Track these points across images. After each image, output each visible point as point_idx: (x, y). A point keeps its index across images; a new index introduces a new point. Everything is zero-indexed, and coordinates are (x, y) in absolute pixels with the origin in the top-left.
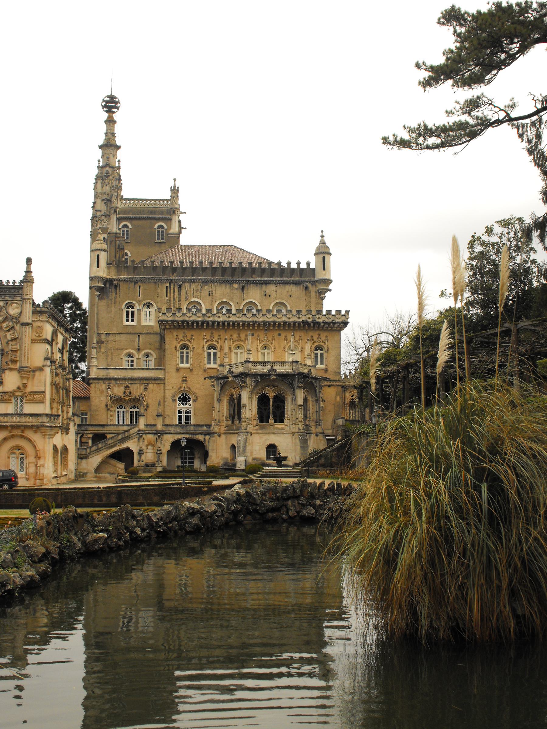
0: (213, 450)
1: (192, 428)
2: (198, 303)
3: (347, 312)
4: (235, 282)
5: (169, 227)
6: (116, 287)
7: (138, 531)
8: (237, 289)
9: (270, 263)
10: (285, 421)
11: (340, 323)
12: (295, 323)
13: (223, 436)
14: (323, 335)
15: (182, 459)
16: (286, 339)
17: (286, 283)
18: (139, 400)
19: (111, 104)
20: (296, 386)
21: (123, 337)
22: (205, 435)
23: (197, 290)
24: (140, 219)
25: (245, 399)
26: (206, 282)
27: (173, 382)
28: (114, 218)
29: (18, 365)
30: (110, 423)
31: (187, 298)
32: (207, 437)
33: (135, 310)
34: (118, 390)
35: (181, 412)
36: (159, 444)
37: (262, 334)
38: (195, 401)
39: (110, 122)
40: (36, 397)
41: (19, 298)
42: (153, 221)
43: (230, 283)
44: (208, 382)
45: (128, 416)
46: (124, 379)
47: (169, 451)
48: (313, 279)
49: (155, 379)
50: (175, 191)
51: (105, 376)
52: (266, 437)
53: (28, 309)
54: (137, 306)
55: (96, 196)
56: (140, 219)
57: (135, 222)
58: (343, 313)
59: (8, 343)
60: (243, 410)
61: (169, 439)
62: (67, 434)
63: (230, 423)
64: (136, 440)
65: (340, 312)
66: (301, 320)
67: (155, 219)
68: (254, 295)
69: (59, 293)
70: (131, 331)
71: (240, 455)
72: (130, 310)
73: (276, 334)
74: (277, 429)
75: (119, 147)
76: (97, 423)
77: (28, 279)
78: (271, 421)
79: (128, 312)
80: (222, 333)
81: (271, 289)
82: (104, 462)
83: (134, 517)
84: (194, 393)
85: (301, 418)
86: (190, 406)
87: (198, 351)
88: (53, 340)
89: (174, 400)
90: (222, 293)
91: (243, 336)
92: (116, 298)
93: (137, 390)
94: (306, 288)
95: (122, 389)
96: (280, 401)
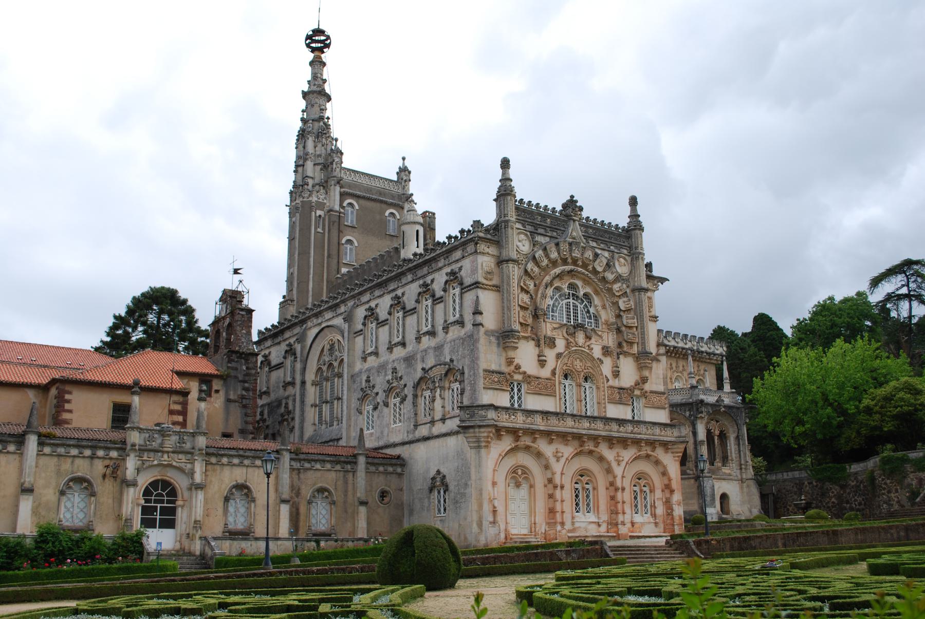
19: (318, 41)
24: (369, 199)
29: (635, 349)
39: (317, 64)
42: (384, 206)
50: (404, 171)
56: (369, 199)
57: (362, 202)
67: (386, 203)
69: (169, 289)
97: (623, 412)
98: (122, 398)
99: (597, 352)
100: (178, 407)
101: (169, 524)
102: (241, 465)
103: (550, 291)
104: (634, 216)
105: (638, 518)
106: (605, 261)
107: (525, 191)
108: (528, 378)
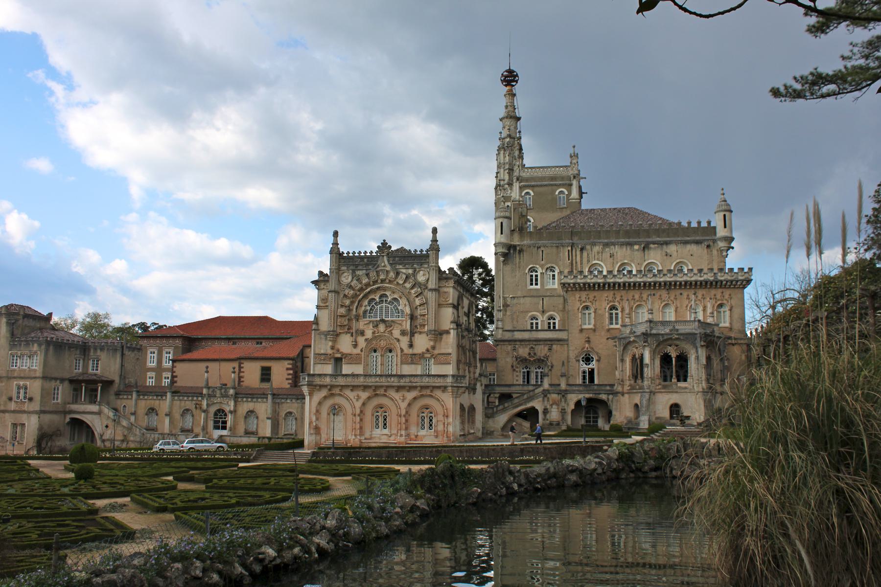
0: (616, 409)
1: (596, 387)
2: (600, 265)
3: (750, 269)
4: (636, 243)
5: (570, 193)
6: (520, 252)
7: (515, 486)
8: (638, 250)
9: (671, 224)
10: (688, 380)
11: (743, 281)
12: (696, 282)
13: (626, 396)
14: (727, 293)
15: (586, 417)
16: (688, 298)
17: (686, 243)
18: (543, 361)
20: (698, 345)
21: (528, 300)
22: (608, 394)
23: (598, 253)
25: (647, 359)
26: (606, 245)
27: (577, 343)
28: (516, 186)
30: (515, 383)
31: (588, 261)
32: (611, 397)
33: (539, 274)
34: (523, 352)
35: (584, 372)
36: (563, 404)
37: (664, 293)
38: (598, 361)
40: (443, 358)
41: (426, 266)
42: (554, 187)
43: (631, 244)
44: (611, 342)
45: (533, 376)
46: (529, 341)
47: (573, 411)
48: (714, 237)
49: (559, 340)
51: (511, 338)
52: (670, 396)
53: (433, 277)
54: (540, 271)
55: (499, 167)
56: (541, 186)
57: (536, 189)
58: (746, 270)
59: (416, 308)
60: (645, 370)
61: (573, 398)
62: (474, 394)
63: (632, 382)
64: (541, 399)
65: (743, 269)
66: (702, 279)
67: (556, 185)
68: (655, 257)
70: (535, 294)
71: (643, 414)
72: (534, 274)
73: (678, 292)
74: (680, 387)
75: (519, 119)
76: (503, 383)
77: (435, 247)
78: (674, 380)
79: (532, 276)
80: (623, 293)
81: (672, 248)
82: (510, 420)
83: (511, 473)
84: (597, 353)
85: (704, 377)
86: (593, 365)
87: (600, 312)
88: (458, 304)
89: (578, 361)
90: (621, 253)
91: (645, 296)
92: (520, 262)
93: (542, 351)
94: (708, 246)
95: (527, 350)
96: (683, 360)
97: (418, 370)
98: (266, 364)
99: (396, 333)
100: (290, 366)
101: (224, 428)
102: (252, 401)
103: (366, 302)
104: (435, 240)
105: (422, 433)
106: (404, 276)
107: (344, 248)
108: (345, 355)
